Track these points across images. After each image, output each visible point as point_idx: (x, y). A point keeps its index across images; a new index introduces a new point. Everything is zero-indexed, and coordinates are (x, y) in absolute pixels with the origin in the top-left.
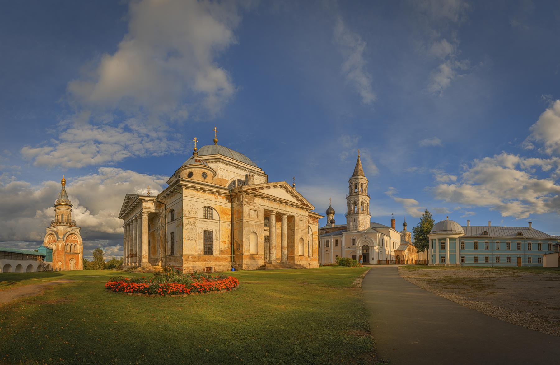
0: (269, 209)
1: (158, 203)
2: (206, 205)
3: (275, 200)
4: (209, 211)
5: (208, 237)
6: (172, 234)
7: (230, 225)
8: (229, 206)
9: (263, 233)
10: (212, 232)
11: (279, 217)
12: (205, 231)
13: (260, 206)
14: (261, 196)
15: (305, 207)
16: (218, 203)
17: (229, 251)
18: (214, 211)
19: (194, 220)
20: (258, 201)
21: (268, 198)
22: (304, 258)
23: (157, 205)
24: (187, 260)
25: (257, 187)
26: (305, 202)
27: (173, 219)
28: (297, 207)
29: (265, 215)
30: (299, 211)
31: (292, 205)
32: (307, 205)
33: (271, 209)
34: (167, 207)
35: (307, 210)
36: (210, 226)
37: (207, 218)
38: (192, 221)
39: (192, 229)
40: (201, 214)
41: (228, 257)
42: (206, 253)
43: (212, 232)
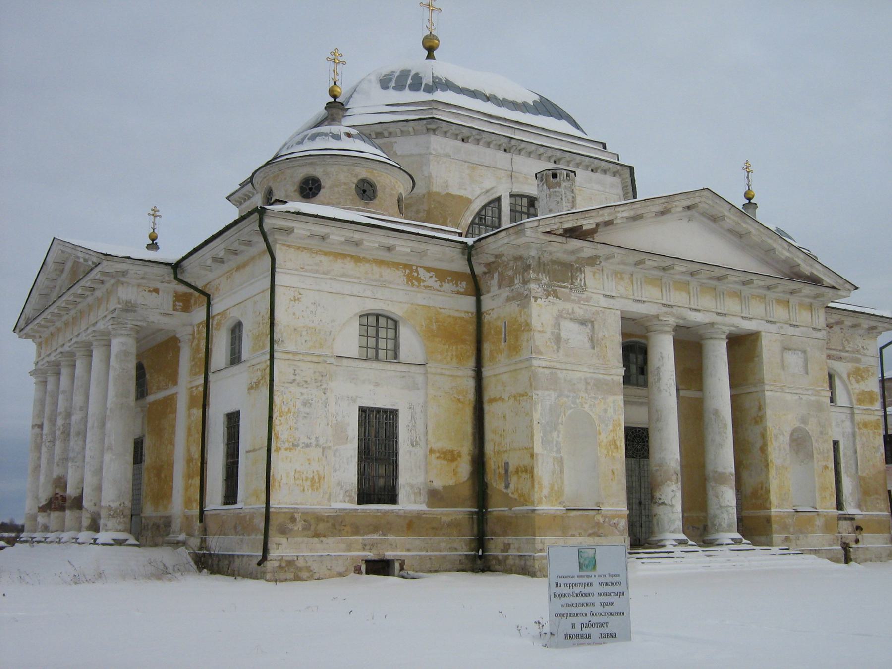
1: (182, 289)
2: (372, 306)
4: (379, 329)
5: (378, 432)
6: (233, 419)
8: (469, 302)
9: (612, 414)
10: (391, 415)
12: (362, 410)
13: (604, 302)
16: (421, 298)
17: (466, 491)
18: (403, 331)
19: (320, 367)
23: (178, 297)
24: (284, 531)
25: (587, 224)
27: (235, 358)
30: (780, 313)
32: (815, 281)
34: (216, 309)
36: (382, 389)
37: (377, 358)
38: (307, 370)
39: (305, 404)
40: (349, 341)
41: (461, 512)
42: (364, 497)
43: (391, 415)
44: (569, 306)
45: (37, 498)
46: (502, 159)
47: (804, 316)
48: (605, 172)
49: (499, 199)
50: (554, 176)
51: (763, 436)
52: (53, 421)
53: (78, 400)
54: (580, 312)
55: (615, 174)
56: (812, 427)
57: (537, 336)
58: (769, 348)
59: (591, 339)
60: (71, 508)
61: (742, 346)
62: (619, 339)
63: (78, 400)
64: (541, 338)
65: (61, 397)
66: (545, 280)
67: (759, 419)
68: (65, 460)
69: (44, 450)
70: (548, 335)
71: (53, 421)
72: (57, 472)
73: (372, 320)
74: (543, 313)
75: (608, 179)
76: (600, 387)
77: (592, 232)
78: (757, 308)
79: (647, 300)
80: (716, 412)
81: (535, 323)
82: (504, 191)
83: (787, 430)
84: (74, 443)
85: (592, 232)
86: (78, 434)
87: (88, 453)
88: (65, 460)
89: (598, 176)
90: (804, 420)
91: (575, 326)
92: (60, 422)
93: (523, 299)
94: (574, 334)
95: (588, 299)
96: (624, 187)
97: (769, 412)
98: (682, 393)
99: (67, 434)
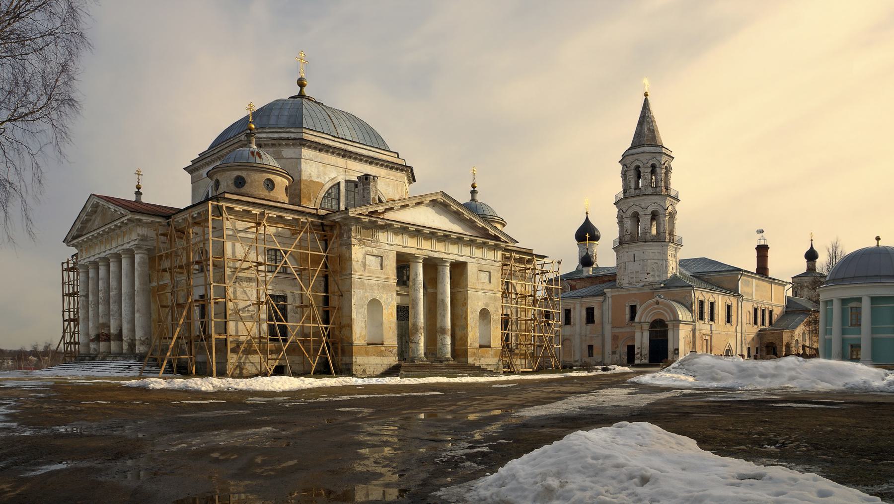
0: (407, 251)
3: (418, 232)
7: (323, 284)
9: (390, 302)
11: (432, 266)
13: (388, 247)
14: (387, 227)
15: (492, 243)
20: (382, 236)
21: (404, 229)
22: (491, 352)
25: (380, 209)
26: (492, 232)
28: (471, 243)
29: (398, 261)
30: (478, 253)
31: (459, 240)
32: (496, 238)
33: (413, 251)
35: (495, 248)
44: (370, 249)
45: (88, 334)
46: (341, 161)
47: (490, 255)
48: (397, 169)
49: (339, 183)
50: (366, 179)
51: (466, 312)
52: (96, 294)
53: (113, 283)
54: (375, 252)
55: (402, 170)
56: (491, 309)
57: (354, 263)
58: (471, 270)
59: (381, 265)
60: (105, 340)
61: (459, 268)
62: (395, 265)
63: (113, 283)
64: (356, 265)
65: (101, 282)
66: (359, 237)
67: (465, 304)
68: (108, 314)
69: (90, 309)
70: (360, 263)
71: (96, 294)
72: (101, 321)
73: (273, 253)
74: (357, 252)
75: (399, 174)
76: (385, 288)
77: (383, 213)
78: (466, 251)
79: (412, 246)
80: (443, 301)
81: (353, 256)
82: (341, 179)
83: (479, 309)
84: (113, 307)
85: (383, 213)
86: (115, 302)
87: (123, 312)
88: (108, 314)
89: (393, 172)
90: (487, 305)
91: (373, 258)
92: (101, 295)
93: (349, 246)
94: (372, 262)
95: (380, 246)
96: (408, 177)
97: (469, 301)
98: (429, 290)
99: (107, 302)
